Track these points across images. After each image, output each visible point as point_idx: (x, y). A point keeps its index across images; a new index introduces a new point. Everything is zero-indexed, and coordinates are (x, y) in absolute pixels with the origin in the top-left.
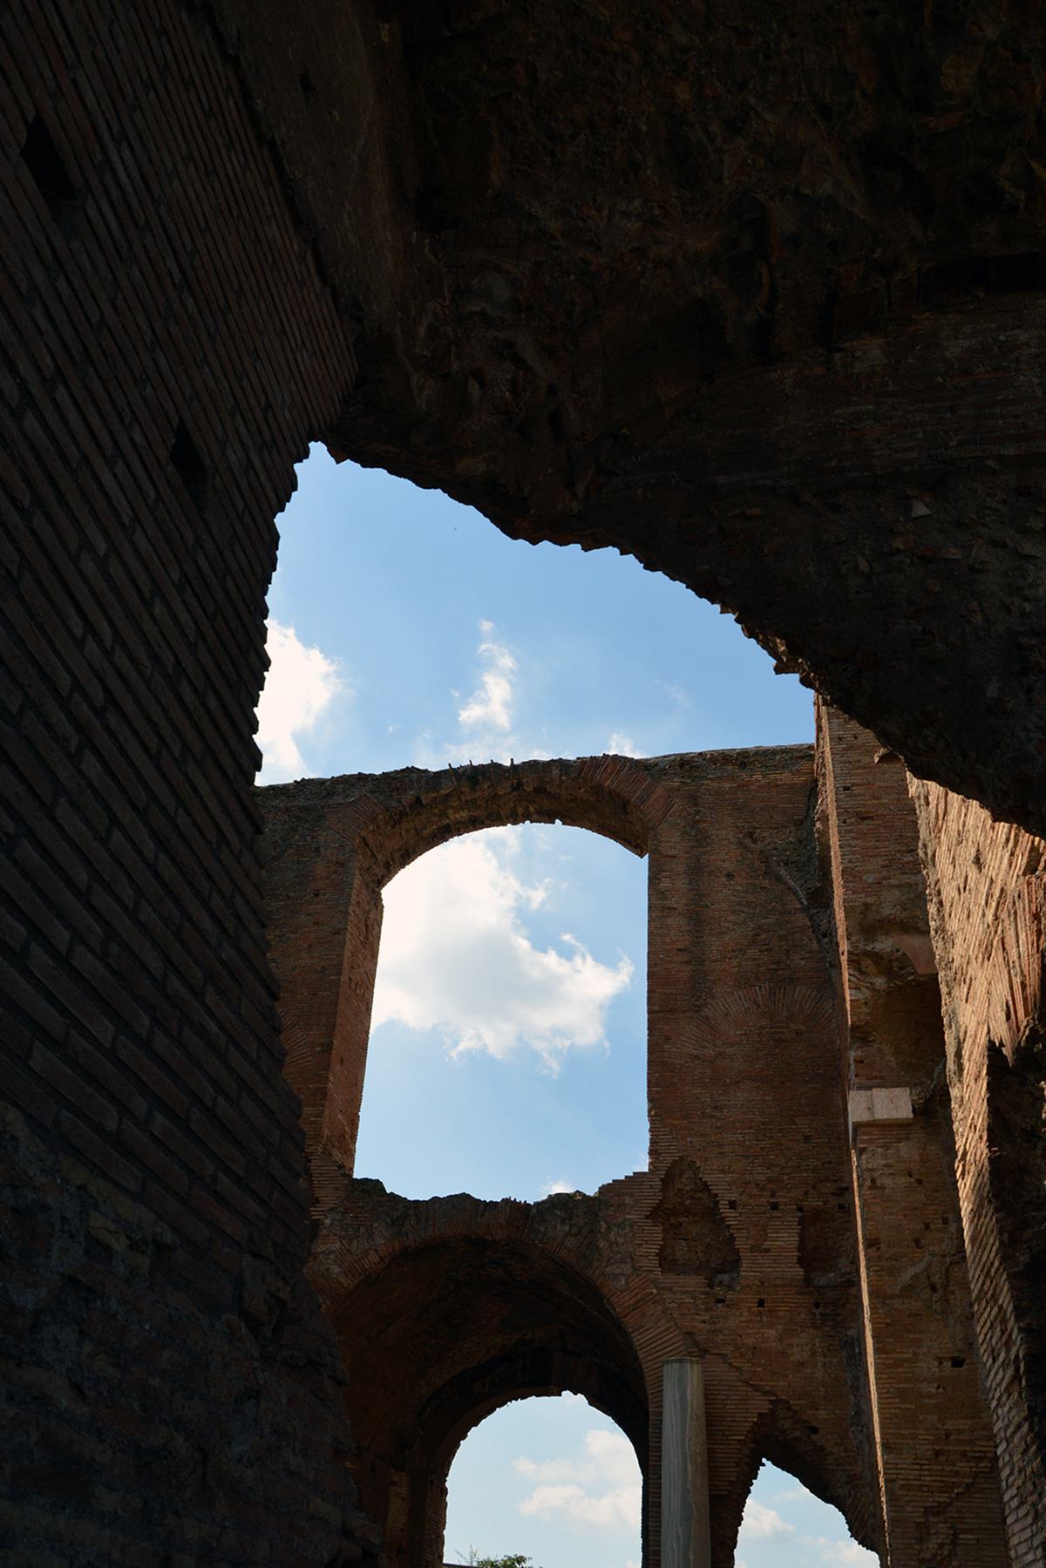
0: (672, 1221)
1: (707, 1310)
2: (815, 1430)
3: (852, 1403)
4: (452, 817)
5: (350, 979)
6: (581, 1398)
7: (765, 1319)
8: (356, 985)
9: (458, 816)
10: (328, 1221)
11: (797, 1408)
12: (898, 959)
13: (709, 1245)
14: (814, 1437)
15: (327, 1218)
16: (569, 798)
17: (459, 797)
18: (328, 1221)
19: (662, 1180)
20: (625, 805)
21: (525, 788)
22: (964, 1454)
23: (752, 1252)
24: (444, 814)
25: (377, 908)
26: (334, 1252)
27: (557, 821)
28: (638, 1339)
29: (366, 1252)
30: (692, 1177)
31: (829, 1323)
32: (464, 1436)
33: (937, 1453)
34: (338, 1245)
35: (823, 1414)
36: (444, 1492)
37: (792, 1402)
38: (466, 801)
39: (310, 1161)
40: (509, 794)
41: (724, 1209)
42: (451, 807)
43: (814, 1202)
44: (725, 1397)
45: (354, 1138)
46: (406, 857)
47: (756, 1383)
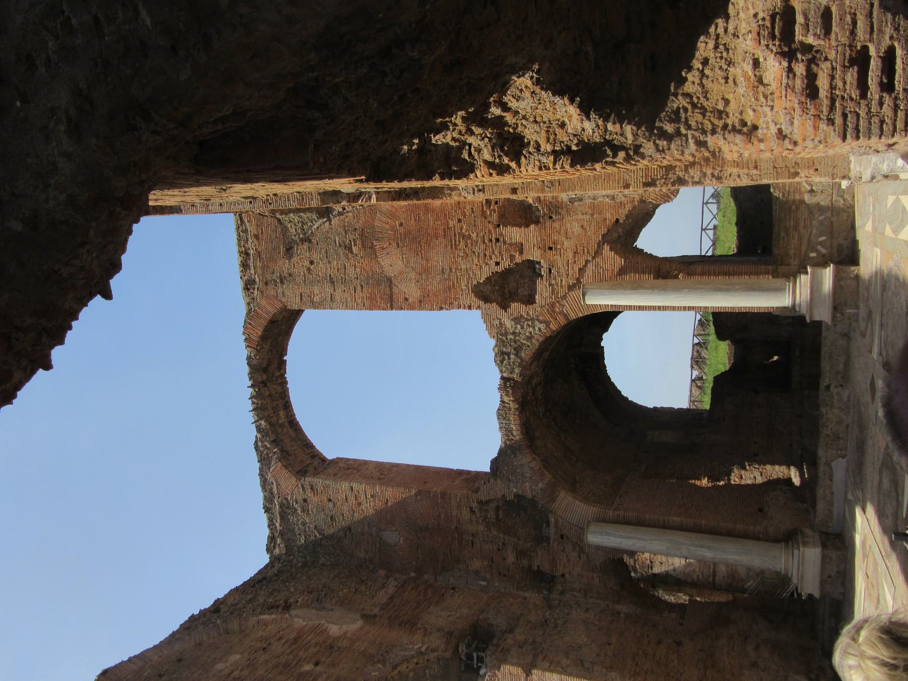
0: (507, 296)
1: (555, 279)
2: (617, 220)
3: (602, 200)
5: (379, 479)
6: (605, 336)
7: (559, 247)
8: (382, 474)
11: (606, 230)
14: (621, 221)
16: (269, 353)
17: (272, 417)
19: (485, 303)
20: (273, 322)
23: (523, 253)
24: (282, 426)
25: (338, 462)
26: (531, 486)
28: (573, 316)
29: (531, 468)
30: (483, 286)
32: (626, 399)
34: (527, 484)
35: (608, 216)
36: (655, 408)
37: (603, 233)
38: (274, 413)
39: (482, 501)
40: (268, 388)
41: (499, 269)
42: (278, 421)
43: (495, 217)
44: (601, 269)
45: (469, 472)
46: (308, 445)
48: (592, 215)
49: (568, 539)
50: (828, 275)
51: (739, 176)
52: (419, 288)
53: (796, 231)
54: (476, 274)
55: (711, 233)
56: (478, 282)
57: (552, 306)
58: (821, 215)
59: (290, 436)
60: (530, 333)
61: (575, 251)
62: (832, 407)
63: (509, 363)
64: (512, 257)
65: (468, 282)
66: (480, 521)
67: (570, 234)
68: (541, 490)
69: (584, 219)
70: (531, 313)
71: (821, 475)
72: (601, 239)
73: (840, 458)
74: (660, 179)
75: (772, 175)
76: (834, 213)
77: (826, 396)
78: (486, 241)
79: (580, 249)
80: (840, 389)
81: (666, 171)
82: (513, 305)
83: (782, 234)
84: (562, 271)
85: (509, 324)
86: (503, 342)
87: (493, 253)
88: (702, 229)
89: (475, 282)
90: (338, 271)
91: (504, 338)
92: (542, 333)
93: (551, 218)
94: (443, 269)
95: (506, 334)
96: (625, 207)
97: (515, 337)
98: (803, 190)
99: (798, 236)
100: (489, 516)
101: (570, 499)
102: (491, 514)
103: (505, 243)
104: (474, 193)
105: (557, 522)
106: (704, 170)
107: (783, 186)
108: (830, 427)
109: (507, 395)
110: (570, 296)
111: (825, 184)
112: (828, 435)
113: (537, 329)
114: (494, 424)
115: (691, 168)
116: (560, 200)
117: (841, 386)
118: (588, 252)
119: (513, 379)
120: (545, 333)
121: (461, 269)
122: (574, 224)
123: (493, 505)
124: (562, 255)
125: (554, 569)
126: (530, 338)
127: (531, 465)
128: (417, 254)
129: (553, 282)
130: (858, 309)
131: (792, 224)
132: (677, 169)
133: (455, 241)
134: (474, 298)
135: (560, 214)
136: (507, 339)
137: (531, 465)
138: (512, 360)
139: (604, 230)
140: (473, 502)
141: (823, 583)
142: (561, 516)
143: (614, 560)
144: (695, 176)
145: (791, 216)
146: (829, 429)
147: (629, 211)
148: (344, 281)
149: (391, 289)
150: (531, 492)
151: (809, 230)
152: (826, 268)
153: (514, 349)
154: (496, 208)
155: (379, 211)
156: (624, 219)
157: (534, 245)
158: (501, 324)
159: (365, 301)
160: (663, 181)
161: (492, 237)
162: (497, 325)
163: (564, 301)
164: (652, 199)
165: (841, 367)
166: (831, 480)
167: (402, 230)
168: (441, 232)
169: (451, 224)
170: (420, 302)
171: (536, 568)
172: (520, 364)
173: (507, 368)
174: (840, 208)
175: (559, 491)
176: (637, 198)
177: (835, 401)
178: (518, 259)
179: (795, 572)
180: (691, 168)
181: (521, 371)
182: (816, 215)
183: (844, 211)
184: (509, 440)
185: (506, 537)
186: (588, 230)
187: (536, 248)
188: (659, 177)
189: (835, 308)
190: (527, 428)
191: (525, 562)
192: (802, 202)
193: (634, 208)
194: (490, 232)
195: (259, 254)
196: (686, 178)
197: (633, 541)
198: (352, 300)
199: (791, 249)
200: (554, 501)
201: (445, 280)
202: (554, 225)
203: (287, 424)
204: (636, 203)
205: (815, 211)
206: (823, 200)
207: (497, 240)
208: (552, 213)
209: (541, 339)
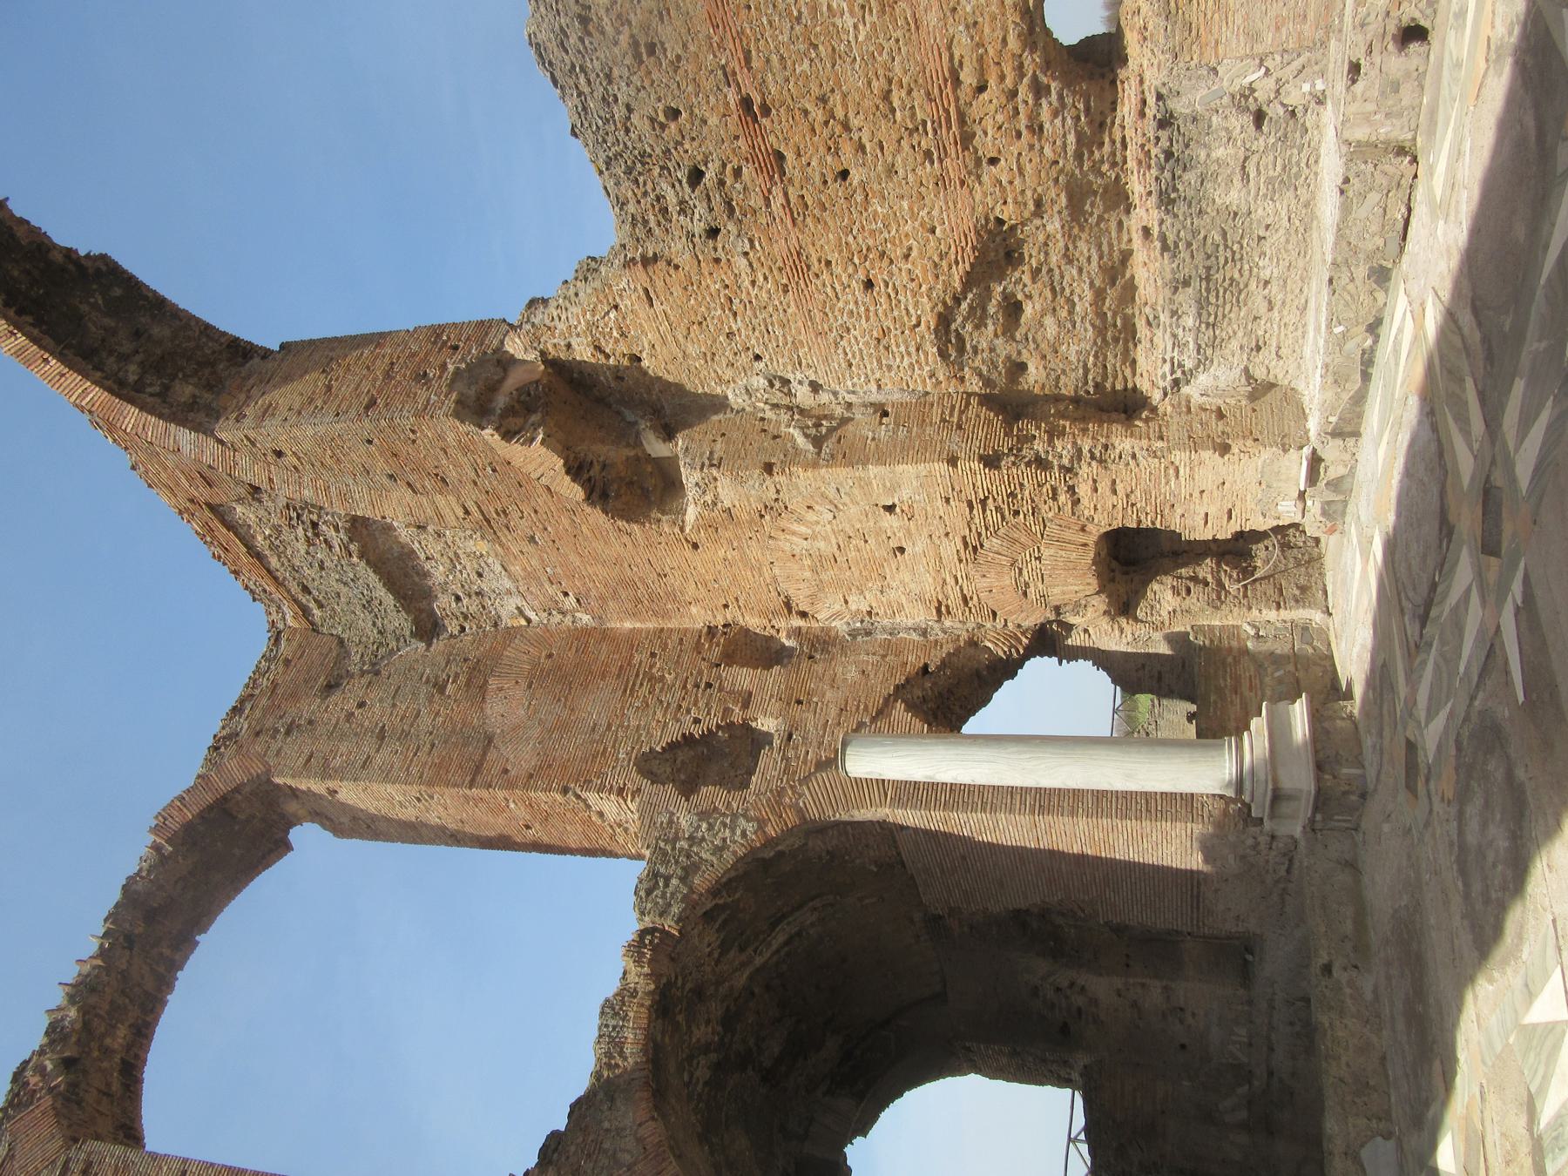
2: (926, 666)
4: (116, 1047)
9: (120, 1041)
12: (520, 395)
14: (932, 668)
19: (652, 783)
21: (136, 932)
22: (961, 412)
23: (748, 708)
24: (107, 1052)
27: (197, 938)
29: (639, 1140)
30: (658, 762)
33: (959, 427)
41: (697, 731)
42: (103, 1036)
43: (717, 652)
50: (1299, 714)
51: (1134, 456)
53: (1236, 694)
57: (780, 793)
58: (1277, 669)
59: (108, 1085)
61: (842, 707)
63: (664, 894)
64: (727, 711)
67: (839, 681)
69: (868, 662)
70: (735, 806)
73: (1379, 1139)
74: (1008, 456)
75: (1187, 446)
76: (1299, 666)
77: (1326, 987)
79: (851, 706)
80: (1354, 973)
81: (1018, 442)
82: (704, 790)
85: (685, 821)
86: (665, 854)
87: (695, 704)
89: (646, 749)
90: (401, 720)
91: (669, 848)
92: (747, 841)
93: (811, 657)
94: (595, 725)
95: (676, 839)
96: (941, 647)
97: (691, 846)
98: (1244, 636)
99: (1241, 699)
103: (721, 689)
104: (702, 469)
106: (1079, 442)
107: (1209, 629)
108: (1344, 1059)
109: (638, 962)
110: (816, 779)
111: (1279, 625)
112: (1341, 1080)
113: (738, 832)
114: (589, 1027)
115: (1058, 439)
116: (833, 634)
117: (1356, 967)
118: (866, 707)
119: (663, 931)
121: (629, 726)
126: (718, 850)
127: (642, 1132)
128: (559, 700)
129: (791, 754)
130: (1363, 767)
131: (1228, 684)
132: (1036, 441)
133: (634, 684)
134: (634, 774)
135: (828, 652)
136: (674, 848)
138: (669, 891)
144: (1064, 452)
145: (1226, 671)
147: (949, 654)
148: (404, 735)
149: (484, 754)
151: (1259, 693)
152: (1294, 702)
153: (683, 868)
154: (722, 641)
155: (522, 635)
157: (772, 696)
158: (671, 822)
159: (426, 770)
160: (1013, 459)
162: (662, 823)
163: (805, 787)
164: (989, 640)
165: (1348, 927)
167: (548, 664)
168: (615, 670)
169: (637, 658)
170: (531, 776)
172: (685, 897)
174: (1308, 659)
176: (965, 636)
177: (1349, 1002)
178: (737, 716)
180: (1058, 439)
183: (1315, 664)
184: (609, 1066)
186: (872, 676)
187: (773, 700)
188: (1006, 451)
189: (1319, 767)
190: (655, 1053)
192: (1246, 651)
193: (958, 650)
194: (700, 673)
195: (275, 687)
196: (1050, 458)
198: (400, 769)
199: (1229, 720)
201: (592, 741)
203: (117, 1058)
204: (962, 644)
206: (1281, 648)
207: (709, 685)
208: (816, 651)
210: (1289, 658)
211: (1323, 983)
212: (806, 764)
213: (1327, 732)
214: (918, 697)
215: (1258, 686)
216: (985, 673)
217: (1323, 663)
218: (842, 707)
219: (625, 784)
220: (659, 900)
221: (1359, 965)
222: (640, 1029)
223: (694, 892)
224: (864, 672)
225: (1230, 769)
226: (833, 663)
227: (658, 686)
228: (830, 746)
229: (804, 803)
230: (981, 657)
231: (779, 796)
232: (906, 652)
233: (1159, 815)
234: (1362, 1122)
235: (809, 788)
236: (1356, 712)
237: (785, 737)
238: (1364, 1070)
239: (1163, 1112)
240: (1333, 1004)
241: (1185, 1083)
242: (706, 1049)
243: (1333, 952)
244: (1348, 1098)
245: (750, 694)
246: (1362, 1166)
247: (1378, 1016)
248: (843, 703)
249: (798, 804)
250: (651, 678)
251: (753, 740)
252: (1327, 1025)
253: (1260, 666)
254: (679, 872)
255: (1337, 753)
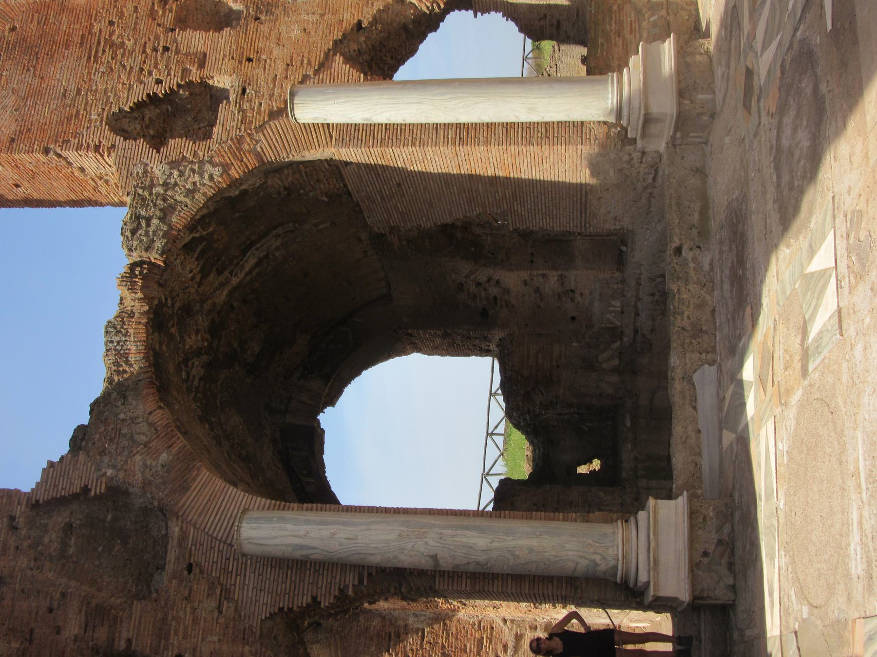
2: (359, 23)
10: (109, 472)
13: (193, 118)
14: (365, 24)
15: (105, 474)
18: (109, 472)
19: (125, 139)
23: (204, 67)
29: (151, 425)
30: (127, 120)
31: (273, 10)
34: (138, 458)
35: (347, 16)
37: (335, 38)
41: (160, 91)
47: (317, 63)
48: (322, 15)
49: (201, 572)
50: (668, 49)
52: (17, 120)
53: (619, 37)
54: (120, 98)
55: (500, 440)
56: (120, 109)
57: (240, 140)
58: (653, 15)
60: (194, 184)
61: (289, 62)
62: (687, 281)
63: (147, 232)
65: (104, 109)
66: (25, 544)
67: (284, 40)
68: (163, 466)
70: (201, 154)
71: (677, 399)
72: (331, 48)
73: (706, 366)
76: (670, 11)
77: (677, 263)
78: (148, 51)
79: (297, 61)
80: (697, 252)
82: (172, 142)
83: (600, 41)
84: (264, 90)
85: (158, 170)
86: (144, 199)
87: (156, 66)
88: (491, 394)
89: (115, 109)
91: (146, 194)
92: (214, 183)
93: (257, 19)
94: (65, 90)
95: (152, 185)
96: (372, 5)
97: (166, 191)
99: (623, 42)
100: (46, 540)
101: (219, 483)
102: (52, 539)
103: (178, 52)
105: (183, 537)
108: (686, 313)
109: (132, 289)
110: (270, 127)
112: (683, 328)
113: (206, 176)
117: (699, 247)
119: (150, 263)
120: (220, 182)
121: (97, 89)
122: (292, 27)
123: (60, 519)
124: (267, 67)
125: (163, 642)
126: (190, 193)
127: (151, 418)
128: (28, 70)
129: (246, 106)
130: (714, 93)
133: (97, 52)
135: (272, 14)
136: (151, 194)
137: (151, 418)
138: (152, 228)
139: (338, 35)
140: (19, 504)
141: (694, 567)
142: (194, 525)
143: (290, 610)
146: (685, 319)
147: (379, 11)
150: (143, 473)
151: (638, 35)
152: (665, 41)
154: (174, 7)
156: (371, 20)
157: (224, 56)
158: (145, 172)
161: (159, 44)
162: (138, 173)
163: (261, 134)
165: (696, 217)
166: (694, 408)
168: (77, 39)
169: (96, 29)
170: (13, 140)
171: (123, 645)
173: (141, 241)
175: (199, 469)
177: (692, 273)
178: (195, 75)
179: (642, 557)
181: (166, 244)
182: (646, 15)
183: (683, 9)
184: (118, 372)
185: (73, 584)
186: (313, 33)
187: (226, 60)
191: (101, 634)
194: (157, 38)
197: (333, 528)
200: (185, 489)
201: (65, 106)
202: (262, 27)
205: (644, 10)
207: (166, 49)
208: (261, 13)
209: (211, 192)
210: (662, 4)
211: (675, 261)
212: (260, 115)
213: (688, 65)
214: (354, 51)
215: (637, 29)
216: (411, 26)
217: (689, 8)
218: (289, 62)
219: (100, 142)
220: (143, 238)
221: (701, 245)
222: (140, 341)
223: (173, 229)
224: (305, 30)
225: (612, 100)
226: (277, 23)
227: (120, 52)
228: (280, 97)
229: (262, 148)
230: (407, 12)
231: (239, 143)
232: (341, 10)
233: (556, 141)
234: (696, 356)
235: (264, 135)
236: (711, 48)
237: (240, 92)
238: (700, 320)
239: (558, 366)
240: (681, 275)
241: (575, 344)
242: (198, 353)
243: (683, 237)
244: (688, 341)
245: (205, 55)
246: (693, 385)
247: (712, 281)
248: (289, 59)
249: (255, 149)
250: (112, 45)
251: (211, 96)
252: (676, 291)
253: (639, 12)
254: (158, 213)
255: (695, 82)
